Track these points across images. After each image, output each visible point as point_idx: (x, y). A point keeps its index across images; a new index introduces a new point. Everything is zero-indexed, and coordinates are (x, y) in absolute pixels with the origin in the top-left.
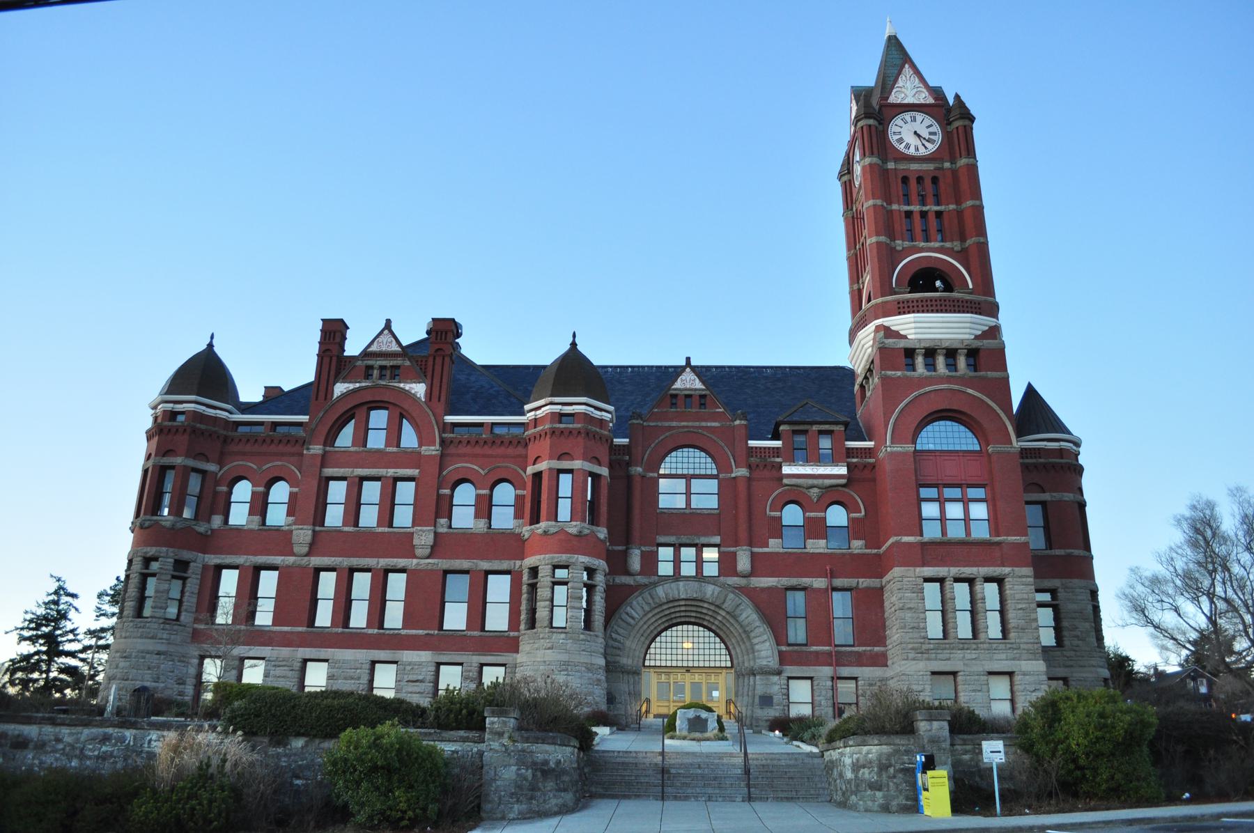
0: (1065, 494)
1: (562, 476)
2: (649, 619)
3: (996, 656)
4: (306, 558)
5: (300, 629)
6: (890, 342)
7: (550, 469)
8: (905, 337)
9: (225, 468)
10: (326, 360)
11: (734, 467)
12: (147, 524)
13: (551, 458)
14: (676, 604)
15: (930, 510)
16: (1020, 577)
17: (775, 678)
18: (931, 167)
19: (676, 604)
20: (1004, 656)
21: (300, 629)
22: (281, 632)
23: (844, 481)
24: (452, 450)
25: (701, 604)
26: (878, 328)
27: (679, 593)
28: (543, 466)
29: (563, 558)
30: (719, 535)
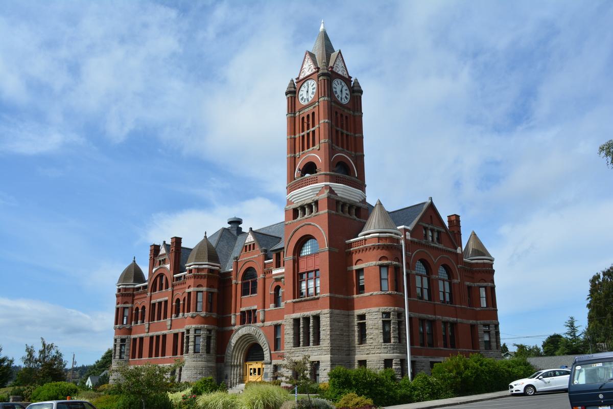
0: (370, 263)
1: (199, 293)
2: (240, 343)
3: (314, 354)
6: (333, 196)
7: (121, 307)
13: (122, 303)
14: (245, 336)
15: (304, 285)
16: (324, 314)
17: (269, 366)
19: (245, 336)
20: (316, 354)
24: (175, 288)
28: (191, 289)
29: (199, 326)
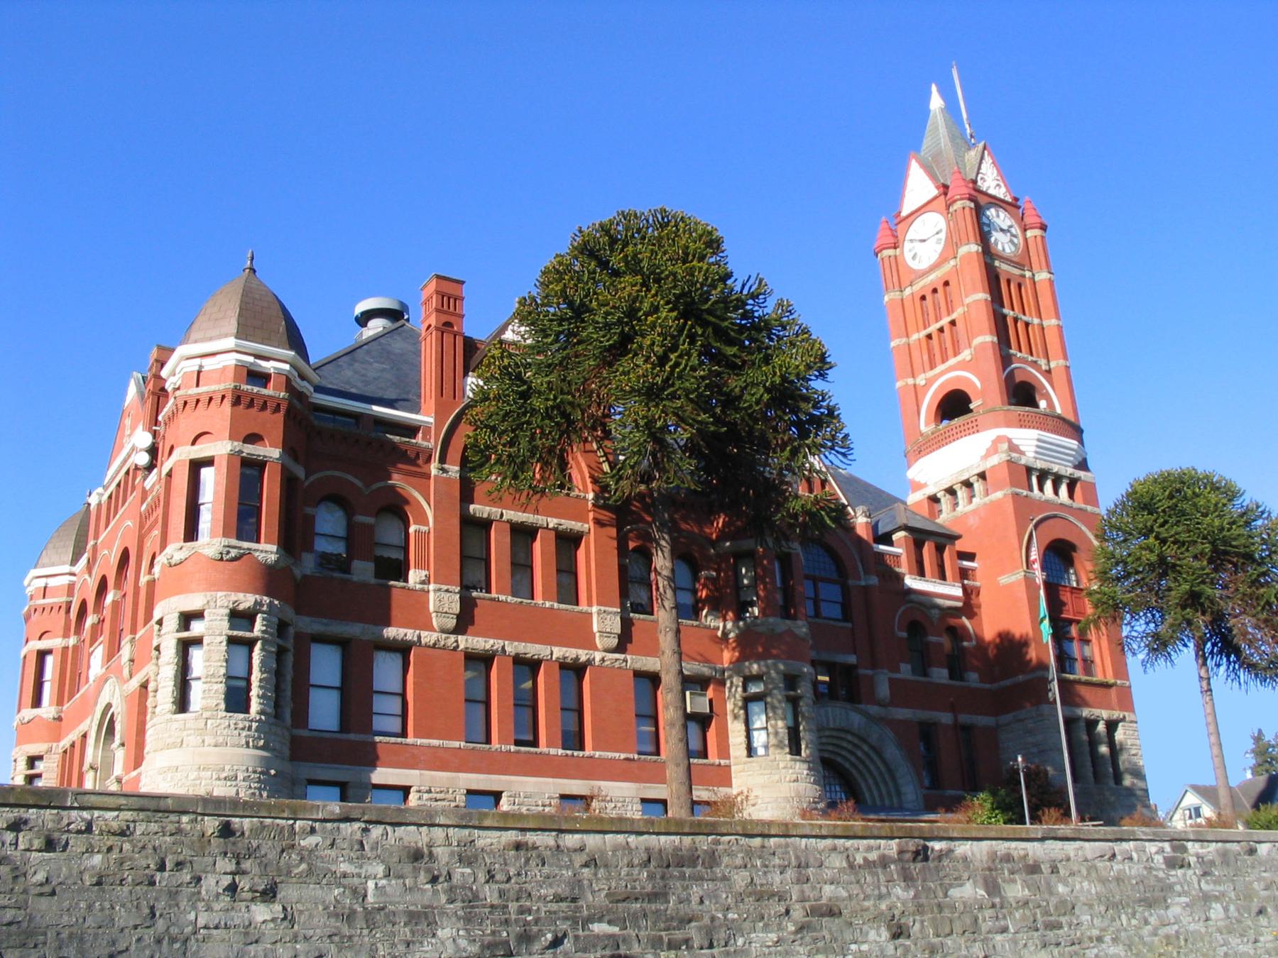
4: (453, 638)
5: (456, 744)
8: (1022, 453)
9: (312, 478)
10: (448, 338)
11: (862, 573)
12: (234, 553)
18: (1017, 272)
21: (456, 744)
22: (429, 747)
23: (960, 604)
25: (843, 735)
26: (999, 439)
27: (828, 721)
30: (855, 653)
